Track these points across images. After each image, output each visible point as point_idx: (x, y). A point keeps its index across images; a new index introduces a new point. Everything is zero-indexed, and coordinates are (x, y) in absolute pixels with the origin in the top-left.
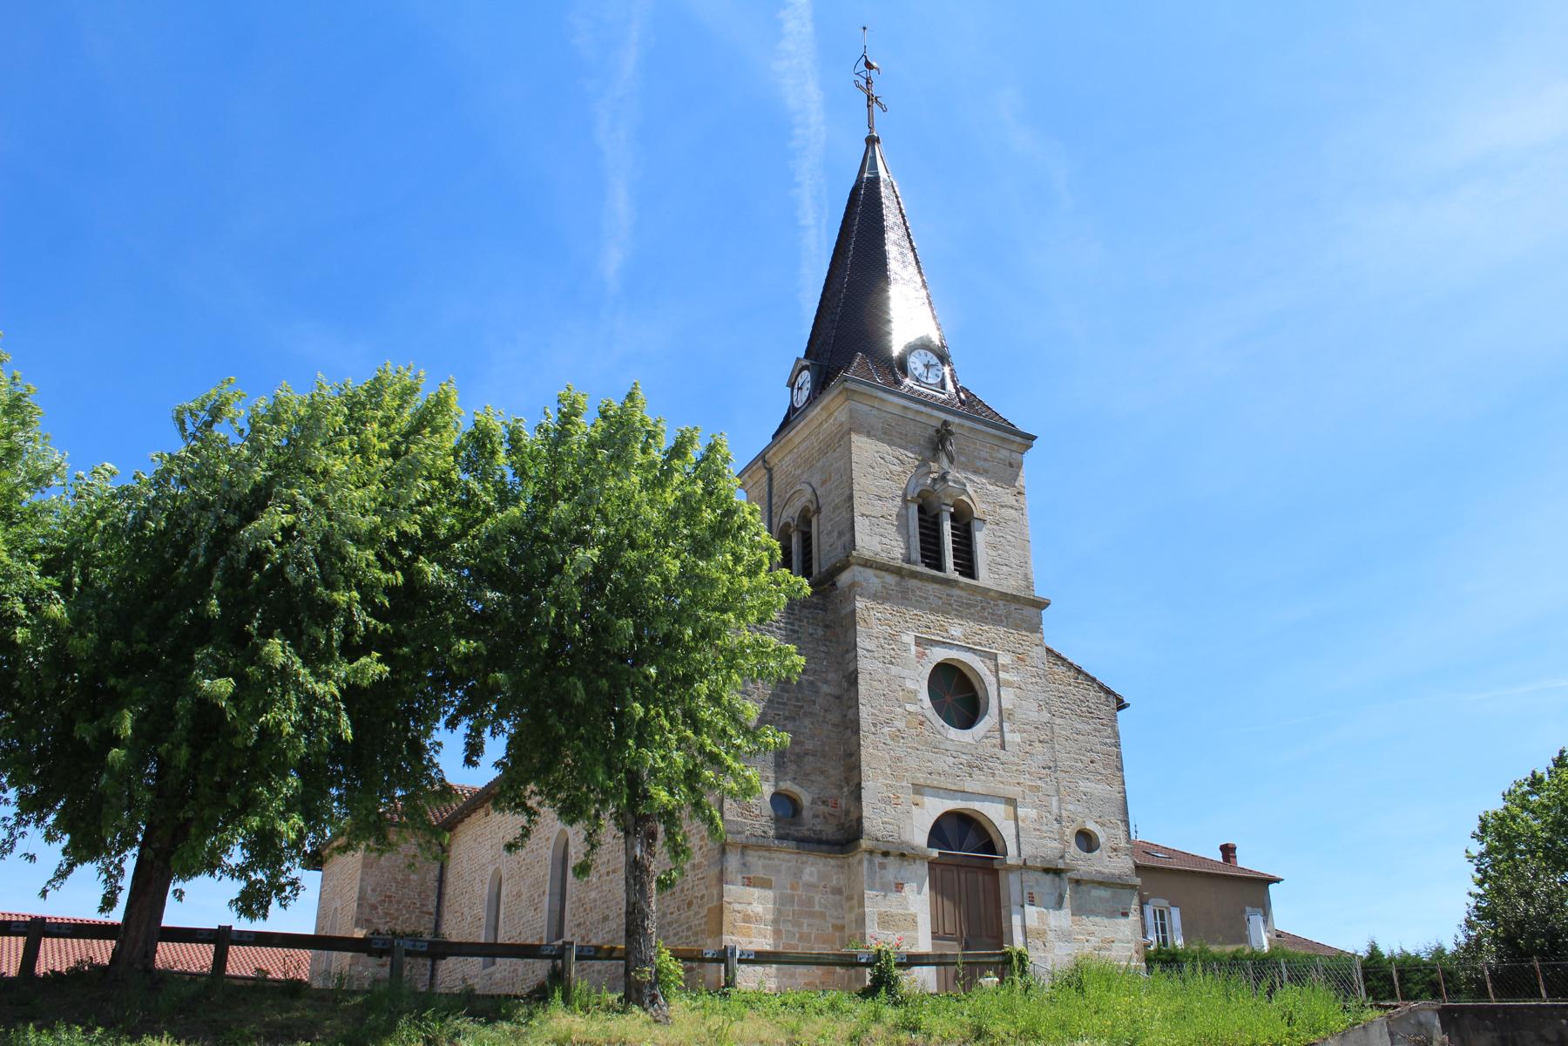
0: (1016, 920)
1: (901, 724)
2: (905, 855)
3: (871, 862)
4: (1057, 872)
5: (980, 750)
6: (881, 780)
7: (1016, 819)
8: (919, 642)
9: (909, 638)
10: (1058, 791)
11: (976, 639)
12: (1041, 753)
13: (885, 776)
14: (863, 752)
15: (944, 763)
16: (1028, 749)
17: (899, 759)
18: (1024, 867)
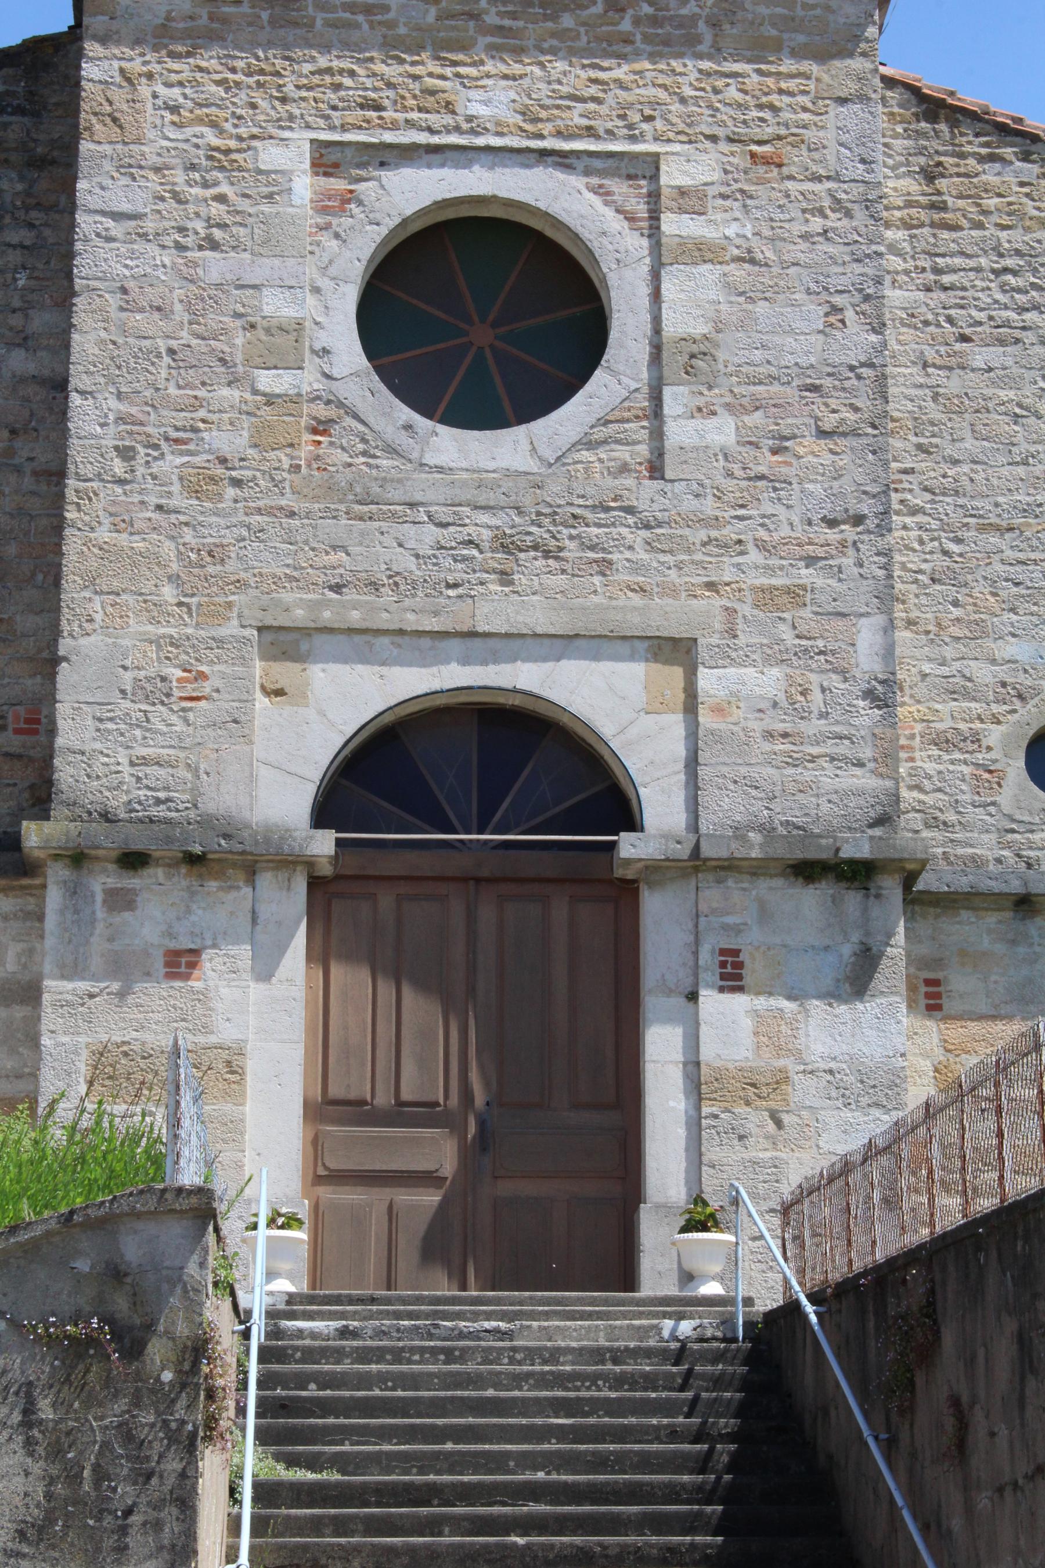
0: (661, 1046)
1: (229, 441)
2: (212, 857)
3: (74, 891)
4: (858, 874)
5: (554, 490)
6: (138, 626)
7: (691, 704)
8: (326, 160)
9: (288, 155)
10: (886, 598)
11: (576, 118)
12: (823, 474)
13: (154, 610)
14: (73, 544)
15: (397, 548)
16: (765, 462)
17: (216, 553)
18: (696, 865)
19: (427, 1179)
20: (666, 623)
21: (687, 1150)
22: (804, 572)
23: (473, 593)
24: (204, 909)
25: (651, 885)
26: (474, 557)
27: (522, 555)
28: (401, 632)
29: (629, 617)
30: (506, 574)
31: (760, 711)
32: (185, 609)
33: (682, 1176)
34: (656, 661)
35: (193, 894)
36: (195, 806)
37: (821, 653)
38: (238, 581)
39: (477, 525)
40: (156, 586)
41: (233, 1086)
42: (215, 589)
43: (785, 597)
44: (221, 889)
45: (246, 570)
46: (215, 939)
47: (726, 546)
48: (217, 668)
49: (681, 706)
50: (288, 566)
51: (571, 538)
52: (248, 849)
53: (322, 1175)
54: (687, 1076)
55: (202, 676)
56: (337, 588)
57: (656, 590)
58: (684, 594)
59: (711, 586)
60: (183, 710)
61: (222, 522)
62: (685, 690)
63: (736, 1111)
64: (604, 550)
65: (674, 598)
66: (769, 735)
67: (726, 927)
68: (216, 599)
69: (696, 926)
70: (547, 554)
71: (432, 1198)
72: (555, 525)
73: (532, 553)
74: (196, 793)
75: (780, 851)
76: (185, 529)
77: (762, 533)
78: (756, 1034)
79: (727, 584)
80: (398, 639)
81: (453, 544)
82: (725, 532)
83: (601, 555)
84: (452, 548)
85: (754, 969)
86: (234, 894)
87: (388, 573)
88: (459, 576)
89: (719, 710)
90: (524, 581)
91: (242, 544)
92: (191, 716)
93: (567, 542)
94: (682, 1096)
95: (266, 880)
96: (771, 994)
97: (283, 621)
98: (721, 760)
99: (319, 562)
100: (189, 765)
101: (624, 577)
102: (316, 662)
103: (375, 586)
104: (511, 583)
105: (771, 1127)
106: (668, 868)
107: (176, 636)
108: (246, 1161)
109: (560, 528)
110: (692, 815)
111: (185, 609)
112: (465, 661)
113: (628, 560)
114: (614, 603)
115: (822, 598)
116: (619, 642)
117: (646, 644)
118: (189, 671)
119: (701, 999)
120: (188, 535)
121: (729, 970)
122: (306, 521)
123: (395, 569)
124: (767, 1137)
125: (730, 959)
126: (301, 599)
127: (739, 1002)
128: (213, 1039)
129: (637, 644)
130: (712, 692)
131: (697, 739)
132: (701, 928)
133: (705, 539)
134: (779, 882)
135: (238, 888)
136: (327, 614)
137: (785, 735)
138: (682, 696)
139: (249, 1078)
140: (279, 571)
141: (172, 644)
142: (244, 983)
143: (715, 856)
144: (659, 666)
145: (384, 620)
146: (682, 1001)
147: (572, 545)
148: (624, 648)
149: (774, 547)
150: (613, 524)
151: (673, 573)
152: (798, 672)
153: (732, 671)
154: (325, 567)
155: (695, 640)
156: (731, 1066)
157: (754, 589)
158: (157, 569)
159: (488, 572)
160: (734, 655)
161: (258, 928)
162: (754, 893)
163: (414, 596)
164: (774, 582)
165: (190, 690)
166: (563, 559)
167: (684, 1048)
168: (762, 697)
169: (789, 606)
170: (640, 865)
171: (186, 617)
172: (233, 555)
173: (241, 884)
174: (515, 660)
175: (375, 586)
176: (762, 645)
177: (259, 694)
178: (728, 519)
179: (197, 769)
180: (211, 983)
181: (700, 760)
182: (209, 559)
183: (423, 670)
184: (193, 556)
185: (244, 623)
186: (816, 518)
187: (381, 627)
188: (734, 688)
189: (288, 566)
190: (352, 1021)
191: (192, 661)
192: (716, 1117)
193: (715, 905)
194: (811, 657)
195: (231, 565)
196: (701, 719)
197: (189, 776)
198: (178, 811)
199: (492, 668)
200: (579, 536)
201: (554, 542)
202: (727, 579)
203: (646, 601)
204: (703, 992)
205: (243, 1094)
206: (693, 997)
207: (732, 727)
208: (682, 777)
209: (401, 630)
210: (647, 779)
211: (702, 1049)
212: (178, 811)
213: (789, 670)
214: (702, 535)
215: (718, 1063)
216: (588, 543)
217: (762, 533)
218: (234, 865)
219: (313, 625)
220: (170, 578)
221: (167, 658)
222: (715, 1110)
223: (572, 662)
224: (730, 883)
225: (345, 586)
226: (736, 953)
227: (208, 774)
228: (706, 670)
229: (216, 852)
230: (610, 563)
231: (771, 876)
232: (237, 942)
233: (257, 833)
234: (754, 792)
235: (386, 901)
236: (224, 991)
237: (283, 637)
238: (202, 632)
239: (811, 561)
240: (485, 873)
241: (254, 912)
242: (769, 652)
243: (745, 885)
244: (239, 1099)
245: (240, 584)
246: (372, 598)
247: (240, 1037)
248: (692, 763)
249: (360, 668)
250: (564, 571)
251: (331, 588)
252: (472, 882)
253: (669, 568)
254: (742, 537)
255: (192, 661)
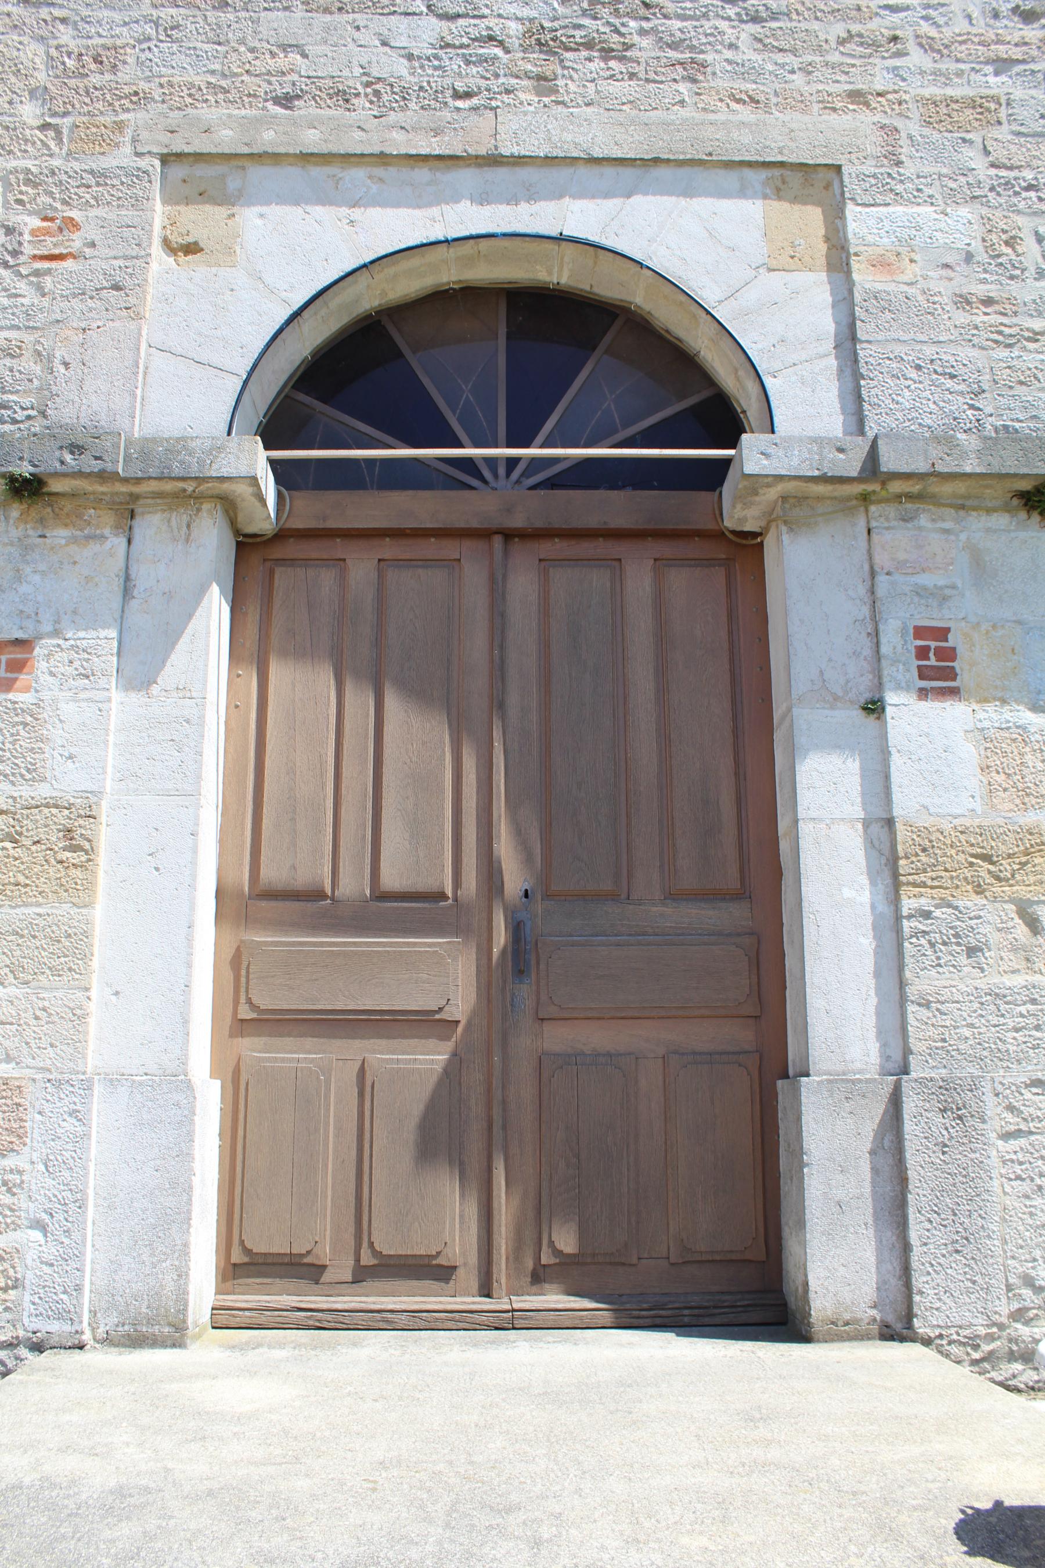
0: (823, 793)
7: (839, 258)
18: (873, 487)
19: (426, 1023)
20: (792, 145)
21: (877, 974)
22: (992, 80)
23: (494, 104)
24: (43, 573)
25: (792, 525)
26: (496, 58)
27: (569, 55)
28: (383, 159)
29: (735, 135)
30: (546, 79)
31: (947, 266)
32: (51, 133)
33: (871, 1021)
34: (780, 198)
35: (27, 549)
36: (43, 414)
37: (1030, 188)
38: (136, 94)
39: (500, 16)
40: (10, 103)
41: (73, 872)
42: (100, 105)
43: (969, 111)
44: (74, 540)
45: (148, 80)
46: (57, 622)
47: (875, 45)
48: (93, 212)
49: (822, 261)
50: (213, 72)
51: (642, 32)
52: (109, 467)
53: (247, 1019)
54: (870, 843)
55: (71, 224)
56: (286, 101)
57: (774, 100)
58: (816, 107)
59: (856, 96)
60: (37, 273)
61: (117, 16)
62: (827, 239)
63: (960, 904)
64: (692, 48)
65: (804, 112)
66: (964, 301)
67: (921, 592)
68: (102, 119)
69: (872, 591)
70: (607, 53)
71: (431, 1057)
72: (619, 17)
73: (584, 53)
74: (47, 393)
75: (1010, 462)
76: (61, 27)
77: (925, 28)
78: (985, 769)
79: (879, 95)
80: (379, 172)
81: (465, 41)
82: (873, 25)
83: (688, 55)
84: (462, 46)
85: (972, 661)
86: (94, 547)
87: (365, 79)
88: (473, 83)
89: (881, 264)
90: (572, 87)
91: (145, 46)
92: (48, 282)
93: (636, 39)
94: (864, 880)
95: (150, 526)
96: (1004, 701)
97: (200, 145)
98: (893, 335)
99: (259, 66)
100: (39, 354)
101: (723, 83)
102: (250, 204)
103: (344, 97)
104: (555, 91)
105: (1021, 931)
106: (819, 498)
107: (34, 169)
108: (92, 1007)
109: (625, 20)
110: (853, 420)
111: (51, 133)
112: (483, 199)
113: (729, 62)
114: (712, 117)
115: (1022, 113)
116: (722, 172)
117: (763, 174)
118: (52, 220)
119: (889, 710)
120: (66, 36)
121: (933, 661)
122: (243, 14)
123: (375, 73)
124: (1014, 950)
125: (933, 644)
126: (230, 116)
127: (952, 717)
128: (44, 791)
129: (748, 173)
130: (870, 239)
131: (852, 305)
132: (881, 591)
133: (845, 35)
134: (1001, 520)
135: (103, 537)
136: (269, 135)
137: (988, 302)
138: (823, 248)
139: (103, 858)
140: (198, 80)
141: (28, 182)
142: (101, 695)
143: (905, 469)
144: (786, 205)
145: (355, 142)
146: (858, 715)
147: (645, 42)
148: (730, 179)
149: (946, 47)
150: (705, 16)
151: (798, 79)
152: (999, 213)
153: (899, 209)
154: (269, 73)
155: (838, 168)
156: (947, 827)
157: (920, 100)
158: (13, 80)
159: (517, 77)
160: (899, 188)
161: (134, 604)
162: (963, 537)
163: (404, 109)
164: (949, 92)
165: (49, 246)
166: (631, 60)
167: (863, 794)
168: (947, 247)
169: (976, 124)
170: (772, 494)
171: (52, 144)
172: (129, 60)
173: (107, 532)
174: (561, 197)
175: (344, 97)
176: (940, 175)
177: (156, 249)
178: (875, 10)
179: (50, 358)
180: (46, 695)
181: (860, 334)
182: (93, 66)
183: (417, 213)
184: (70, 63)
185: (140, 149)
186: (1005, 8)
187: (351, 151)
188: (905, 234)
189: (213, 72)
190: (302, 759)
191: (58, 205)
192: (927, 915)
193: (901, 556)
194: (1016, 194)
195: (125, 74)
196: (855, 276)
197: (37, 369)
198: (15, 422)
199: (524, 207)
200: (654, 30)
201: (616, 38)
202: (879, 88)
203: (761, 115)
204: (891, 698)
205: (90, 886)
206: (874, 707)
207: (906, 288)
208: (832, 362)
209: (382, 153)
210: (777, 365)
211: (897, 796)
212: (15, 422)
213: (984, 211)
214: (839, 29)
215: (924, 821)
216: (667, 39)
217: (925, 28)
218: (98, 501)
219: (246, 150)
220: (32, 93)
221: (19, 202)
222: (924, 903)
223: (650, 198)
224: (923, 521)
225: (298, 97)
226: (942, 633)
227: (66, 365)
228: (859, 209)
229: (56, 475)
230: (704, 65)
231: (989, 511)
232: (94, 623)
233: (129, 443)
234: (949, 383)
235: (361, 567)
236: (68, 709)
237: (203, 171)
238: (76, 166)
239: (1002, 65)
240: (518, 521)
241: (128, 578)
242: (953, 185)
243: (947, 525)
244: (82, 893)
245: (139, 99)
246: (341, 111)
247: (89, 786)
248: (848, 341)
249: (319, 211)
250: (632, 76)
251: (277, 101)
252: (498, 541)
253: (793, 72)
254: (898, 33)
255: (58, 205)
